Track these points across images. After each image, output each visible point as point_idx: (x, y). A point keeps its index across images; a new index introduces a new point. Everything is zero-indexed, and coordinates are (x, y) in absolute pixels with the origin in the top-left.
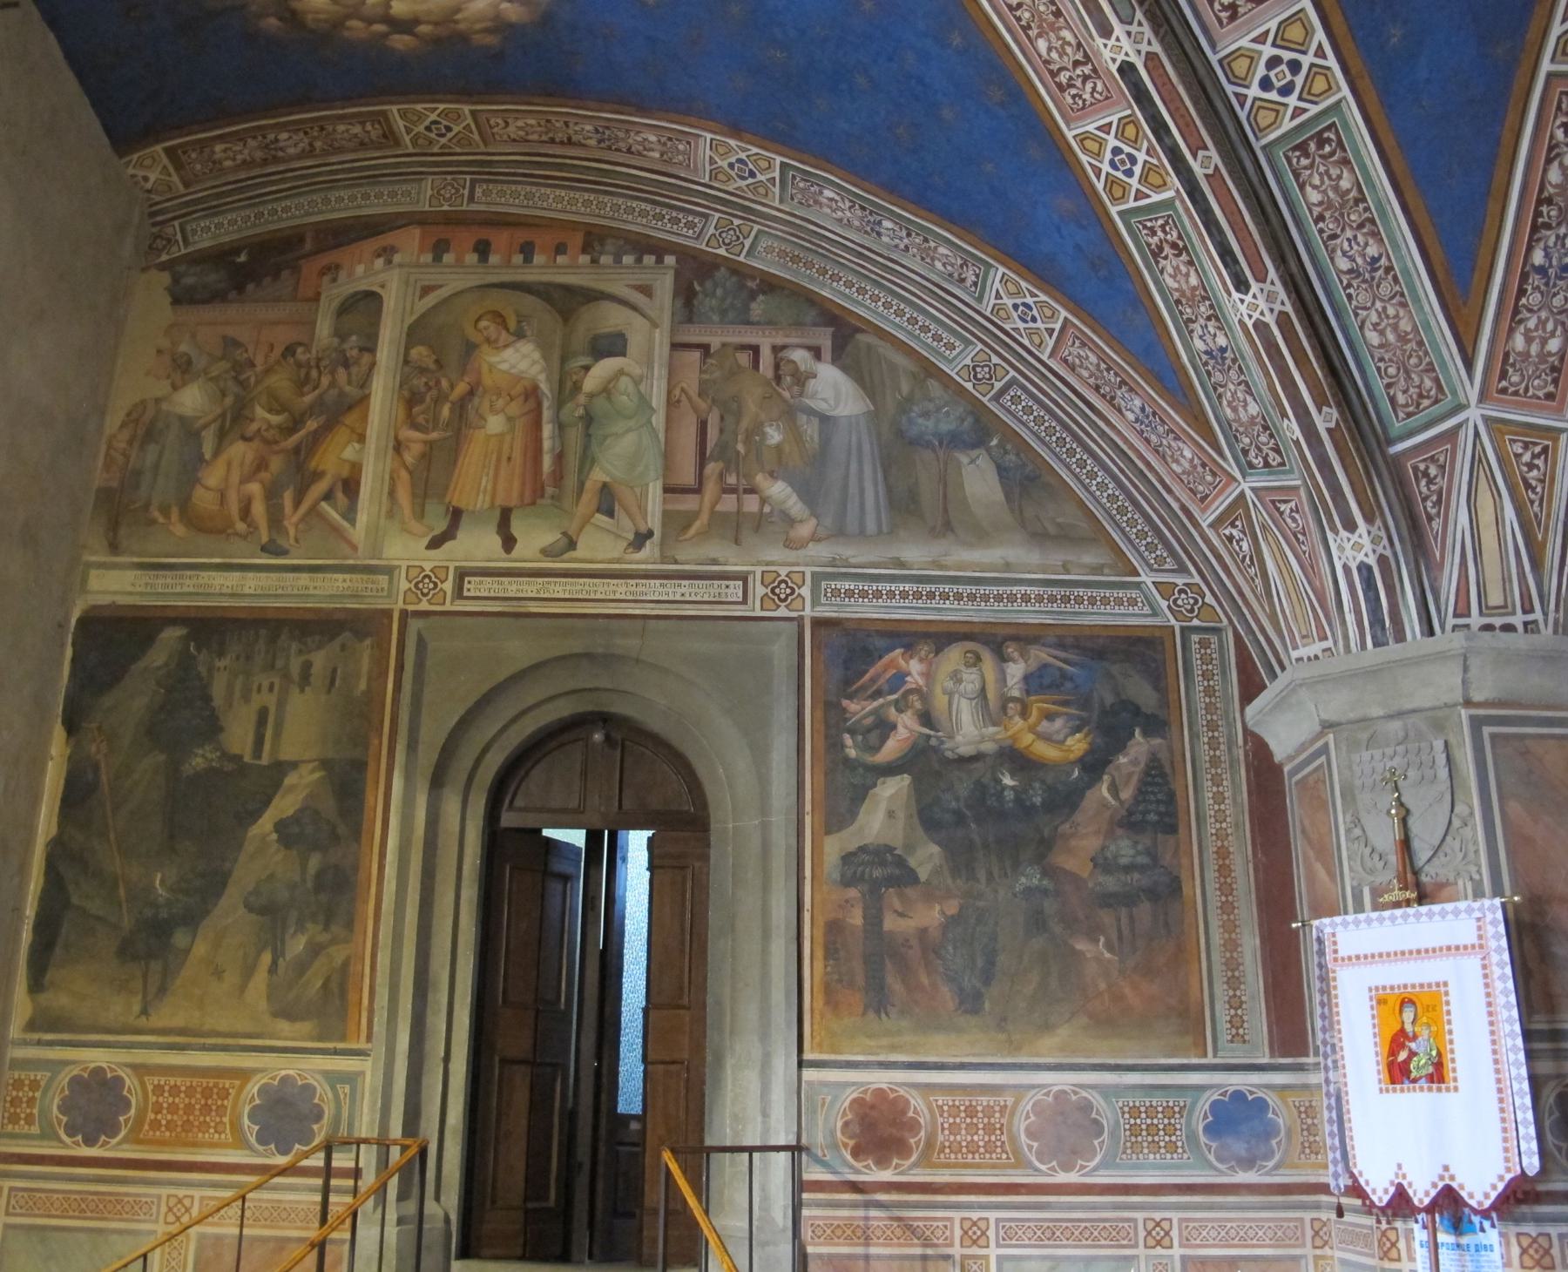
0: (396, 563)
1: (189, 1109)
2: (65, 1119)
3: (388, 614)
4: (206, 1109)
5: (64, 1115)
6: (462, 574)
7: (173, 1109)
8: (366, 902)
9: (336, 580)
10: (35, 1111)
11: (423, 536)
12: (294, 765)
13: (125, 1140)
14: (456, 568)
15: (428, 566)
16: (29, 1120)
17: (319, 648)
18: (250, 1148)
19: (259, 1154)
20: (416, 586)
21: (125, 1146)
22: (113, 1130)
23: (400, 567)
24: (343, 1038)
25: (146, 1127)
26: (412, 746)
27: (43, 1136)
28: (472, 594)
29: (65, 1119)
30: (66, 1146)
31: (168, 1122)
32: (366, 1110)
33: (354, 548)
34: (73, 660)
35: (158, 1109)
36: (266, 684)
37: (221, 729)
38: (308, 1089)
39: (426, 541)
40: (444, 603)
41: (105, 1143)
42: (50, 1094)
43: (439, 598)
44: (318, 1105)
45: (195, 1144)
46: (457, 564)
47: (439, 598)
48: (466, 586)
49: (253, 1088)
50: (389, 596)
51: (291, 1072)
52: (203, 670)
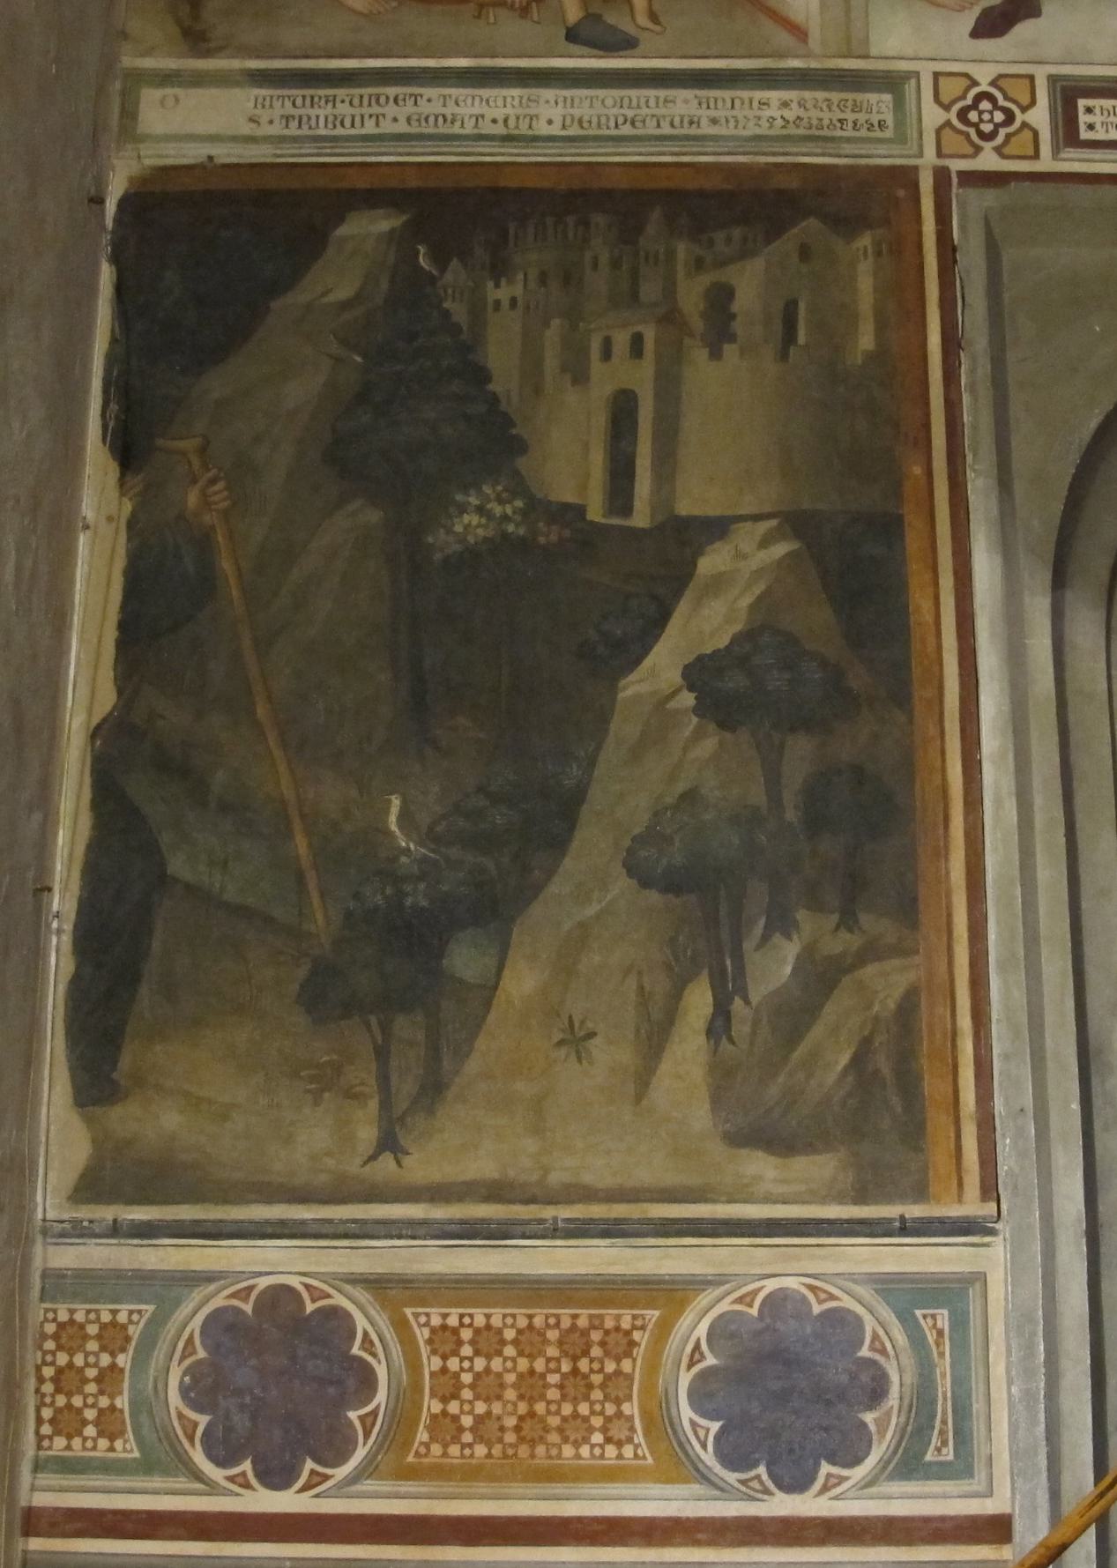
0: (903, 66)
1: (531, 1385)
2: (203, 1420)
3: (906, 177)
4: (576, 1387)
5: (199, 1408)
6: (1068, 95)
7: (488, 1387)
8: (943, 853)
9: (764, 104)
10: (122, 1402)
11: (962, 9)
12: (717, 528)
13: (368, 1470)
14: (1053, 80)
15: (984, 76)
16: (109, 1425)
17: (745, 253)
18: (704, 1477)
19: (723, 1490)
20: (963, 115)
21: (369, 1485)
22: (334, 1448)
23: (917, 74)
24: (920, 1193)
25: (422, 1435)
26: (1004, 483)
27: (147, 1466)
28: (1099, 135)
29: (203, 1420)
30: (212, 1488)
31: (479, 1420)
32: (998, 1369)
33: (800, 33)
34: (120, 289)
35: (449, 1388)
36: (621, 340)
37: (519, 447)
38: (839, 1320)
39: (969, 20)
40: (1036, 156)
41: (316, 1479)
42: (159, 1354)
43: (1023, 142)
44: (873, 1363)
45: (551, 1475)
46: (1054, 70)
47: (1023, 142)
48: (1083, 118)
49: (695, 1325)
50: (901, 138)
51: (792, 1283)
52: (458, 311)
